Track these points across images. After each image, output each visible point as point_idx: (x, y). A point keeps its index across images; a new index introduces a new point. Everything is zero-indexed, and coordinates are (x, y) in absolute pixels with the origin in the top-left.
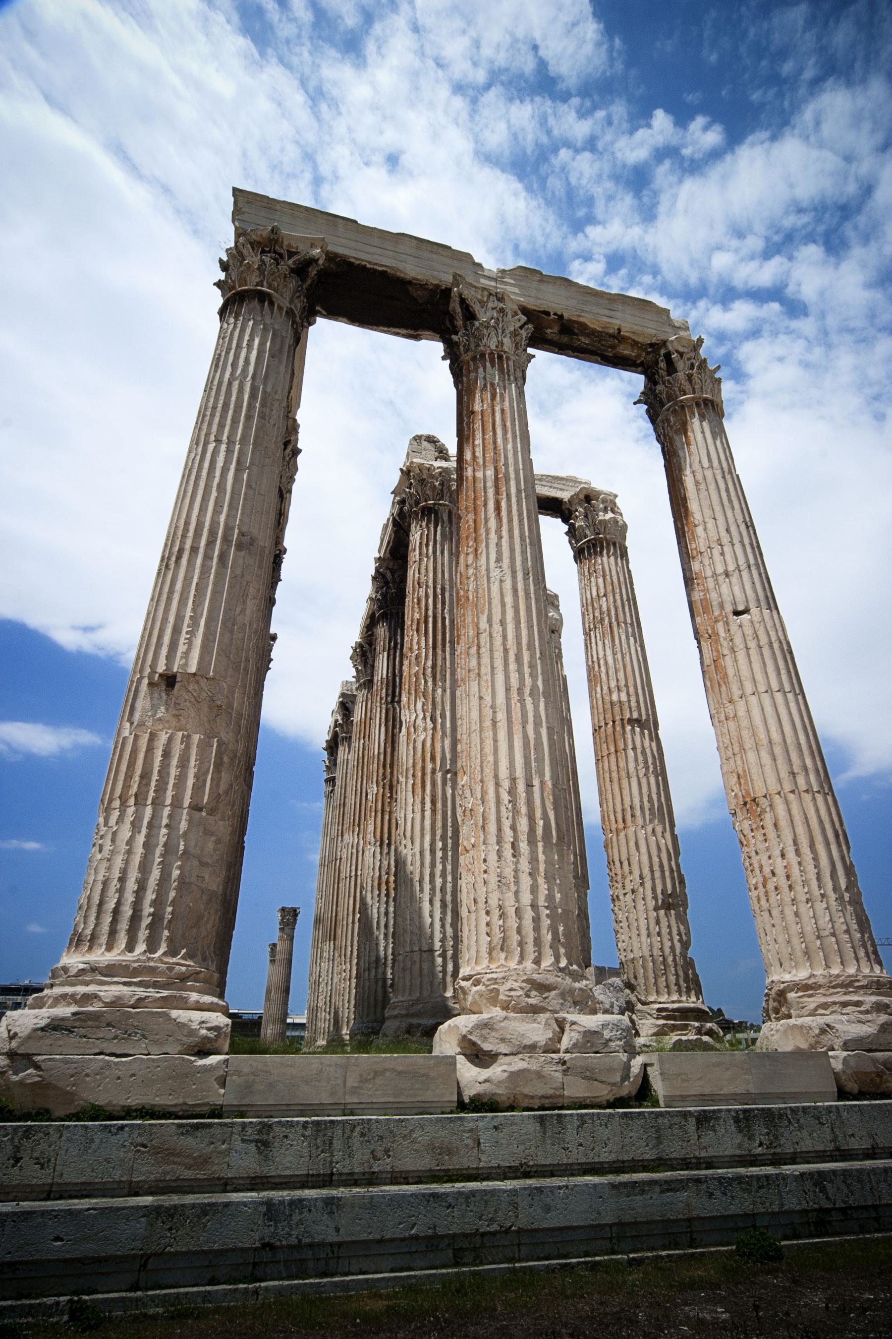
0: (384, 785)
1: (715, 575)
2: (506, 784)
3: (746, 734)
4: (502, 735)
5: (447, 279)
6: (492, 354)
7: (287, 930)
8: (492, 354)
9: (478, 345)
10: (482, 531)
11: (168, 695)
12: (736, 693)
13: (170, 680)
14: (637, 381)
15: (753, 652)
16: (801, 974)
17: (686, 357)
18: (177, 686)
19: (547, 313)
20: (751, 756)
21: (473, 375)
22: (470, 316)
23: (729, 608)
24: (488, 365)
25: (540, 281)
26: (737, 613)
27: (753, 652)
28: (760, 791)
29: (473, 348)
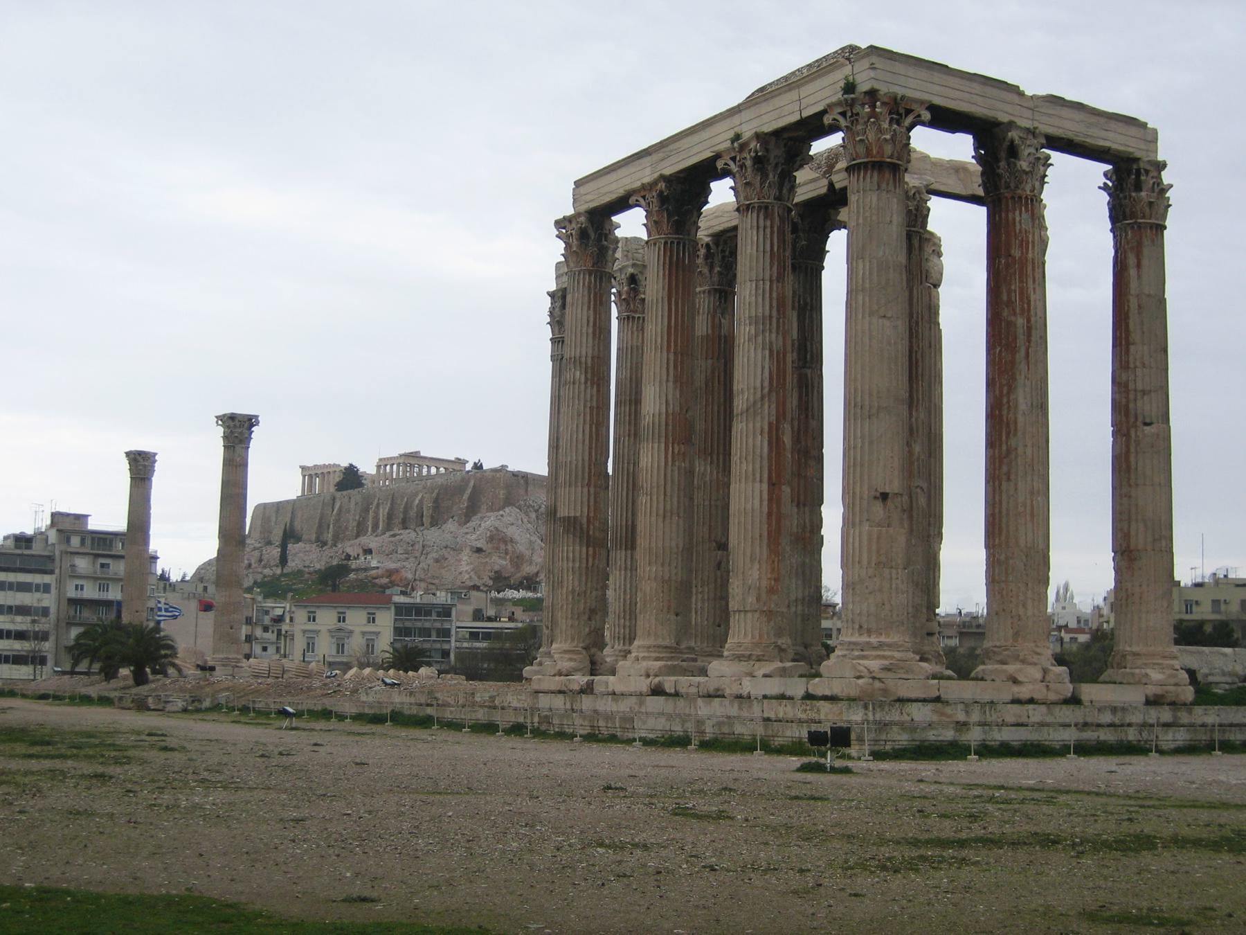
1: (1135, 390)
5: (1004, 118)
6: (1026, 197)
7: (238, 448)
8: (1026, 197)
9: (1017, 187)
11: (884, 504)
12: (1132, 482)
13: (884, 496)
16: (1135, 649)
17: (1151, 174)
18: (889, 502)
19: (1063, 139)
20: (1133, 523)
21: (1010, 215)
22: (1013, 152)
24: (1023, 208)
25: (1063, 106)
26: (1146, 424)
29: (1013, 188)
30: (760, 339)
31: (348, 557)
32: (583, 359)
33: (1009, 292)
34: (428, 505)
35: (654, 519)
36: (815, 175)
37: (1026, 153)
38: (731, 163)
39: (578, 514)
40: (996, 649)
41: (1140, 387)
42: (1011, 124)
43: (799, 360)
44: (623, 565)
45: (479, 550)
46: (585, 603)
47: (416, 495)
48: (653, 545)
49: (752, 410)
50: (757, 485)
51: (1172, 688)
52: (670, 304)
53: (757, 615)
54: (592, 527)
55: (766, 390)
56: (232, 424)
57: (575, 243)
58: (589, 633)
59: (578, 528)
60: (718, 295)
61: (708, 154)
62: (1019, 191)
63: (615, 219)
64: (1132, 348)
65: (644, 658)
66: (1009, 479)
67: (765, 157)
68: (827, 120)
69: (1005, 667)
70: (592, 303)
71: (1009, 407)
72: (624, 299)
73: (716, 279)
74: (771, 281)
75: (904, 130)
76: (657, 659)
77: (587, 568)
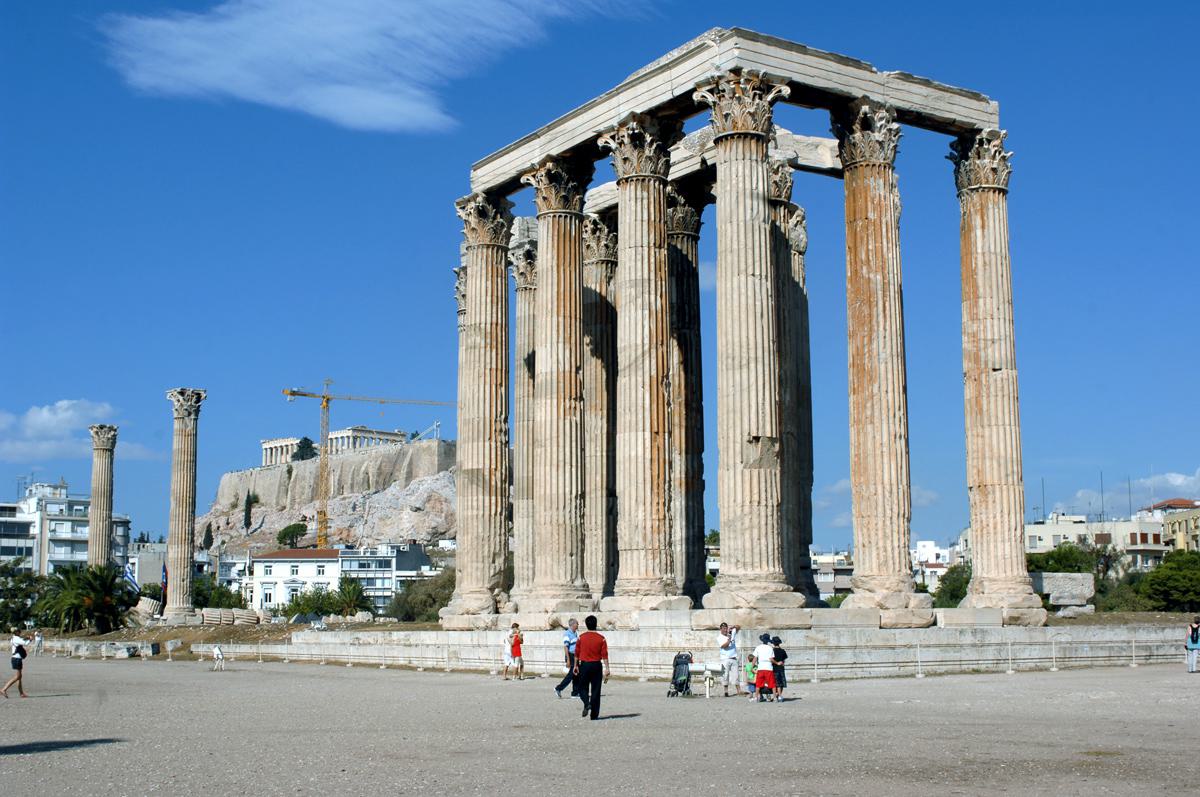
0: (680, 403)
1: (985, 340)
2: (888, 487)
3: (987, 449)
4: (886, 460)
5: (858, 93)
10: (874, 323)
13: (757, 439)
14: (955, 138)
15: (999, 399)
16: (992, 575)
19: (912, 112)
20: (988, 463)
22: (867, 125)
23: (990, 366)
26: (994, 370)
27: (999, 399)
28: (989, 482)
30: (639, 301)
31: (305, 518)
32: (483, 326)
33: (868, 250)
34: (372, 471)
35: (548, 468)
36: (688, 154)
37: (879, 125)
38: (611, 141)
39: (481, 467)
40: (863, 578)
41: (989, 337)
42: (865, 99)
43: (678, 321)
44: (526, 514)
45: (418, 509)
46: (489, 547)
47: (362, 463)
48: (548, 491)
49: (633, 367)
50: (640, 434)
51: (1025, 611)
52: (558, 272)
53: (643, 553)
54: (493, 477)
55: (647, 347)
56: (181, 398)
57: (473, 220)
58: (494, 576)
59: (481, 478)
60: (604, 265)
61: (590, 134)
62: (873, 160)
63: (510, 198)
64: (981, 301)
65: (543, 596)
66: (872, 423)
67: (640, 133)
68: (696, 97)
69: (872, 594)
70: (490, 274)
71: (870, 356)
72: (522, 274)
73: (603, 251)
74: (649, 247)
75: (766, 104)
76: (554, 597)
77: (490, 515)
